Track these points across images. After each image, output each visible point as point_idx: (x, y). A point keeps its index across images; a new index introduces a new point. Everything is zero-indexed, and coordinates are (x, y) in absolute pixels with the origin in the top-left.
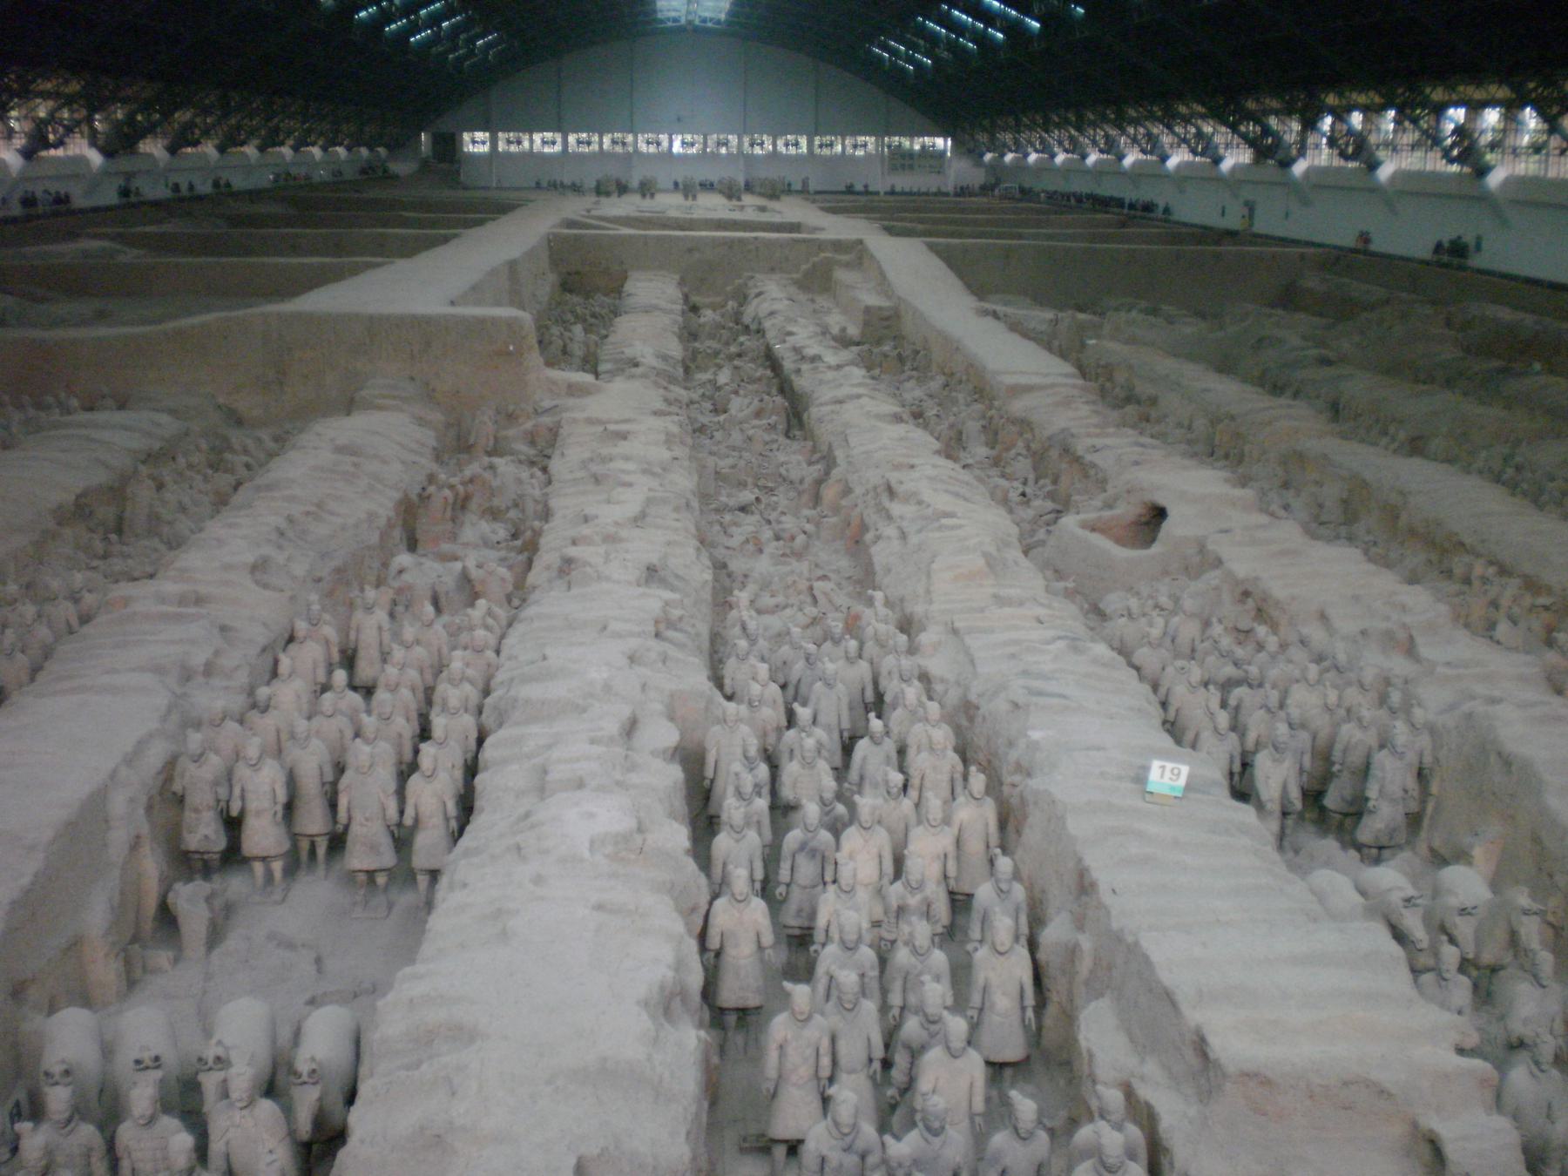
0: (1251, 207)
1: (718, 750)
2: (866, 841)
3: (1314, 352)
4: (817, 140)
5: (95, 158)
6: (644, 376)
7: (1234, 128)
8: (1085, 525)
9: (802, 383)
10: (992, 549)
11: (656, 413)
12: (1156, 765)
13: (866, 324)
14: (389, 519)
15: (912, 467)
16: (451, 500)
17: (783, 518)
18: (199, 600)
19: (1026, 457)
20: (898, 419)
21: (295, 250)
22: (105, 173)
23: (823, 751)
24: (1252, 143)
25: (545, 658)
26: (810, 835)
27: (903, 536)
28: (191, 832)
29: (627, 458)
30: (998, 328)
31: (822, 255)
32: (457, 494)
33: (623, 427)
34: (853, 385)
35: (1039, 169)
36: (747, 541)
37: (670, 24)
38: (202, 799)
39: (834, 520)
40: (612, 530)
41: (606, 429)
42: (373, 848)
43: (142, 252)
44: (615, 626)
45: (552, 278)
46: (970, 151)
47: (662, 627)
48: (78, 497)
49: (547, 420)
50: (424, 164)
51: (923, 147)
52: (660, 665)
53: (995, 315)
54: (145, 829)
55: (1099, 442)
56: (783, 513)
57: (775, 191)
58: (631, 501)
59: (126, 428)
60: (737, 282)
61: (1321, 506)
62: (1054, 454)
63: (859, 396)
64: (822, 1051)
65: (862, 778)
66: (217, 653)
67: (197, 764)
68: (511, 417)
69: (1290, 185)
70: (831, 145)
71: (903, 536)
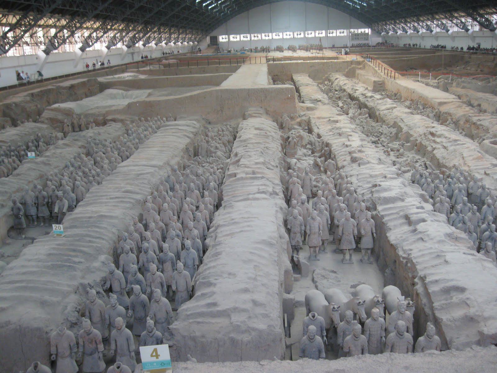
5: (125, 48)
7: (475, 19)
8: (491, 143)
9: (370, 104)
11: (338, 115)
13: (374, 86)
15: (434, 127)
17: (389, 145)
19: (452, 124)
20: (412, 113)
21: (191, 73)
22: (128, 53)
24: (481, 24)
25: (380, 185)
27: (445, 147)
29: (345, 128)
30: (421, 84)
31: (352, 66)
34: (390, 104)
38: (297, 229)
39: (409, 144)
40: (359, 149)
41: (330, 120)
42: (351, 243)
44: (389, 176)
46: (378, 32)
49: (304, 118)
50: (209, 46)
53: (418, 81)
55: (481, 118)
57: (320, 48)
62: (462, 123)
63: (395, 108)
68: (292, 118)
71: (445, 147)
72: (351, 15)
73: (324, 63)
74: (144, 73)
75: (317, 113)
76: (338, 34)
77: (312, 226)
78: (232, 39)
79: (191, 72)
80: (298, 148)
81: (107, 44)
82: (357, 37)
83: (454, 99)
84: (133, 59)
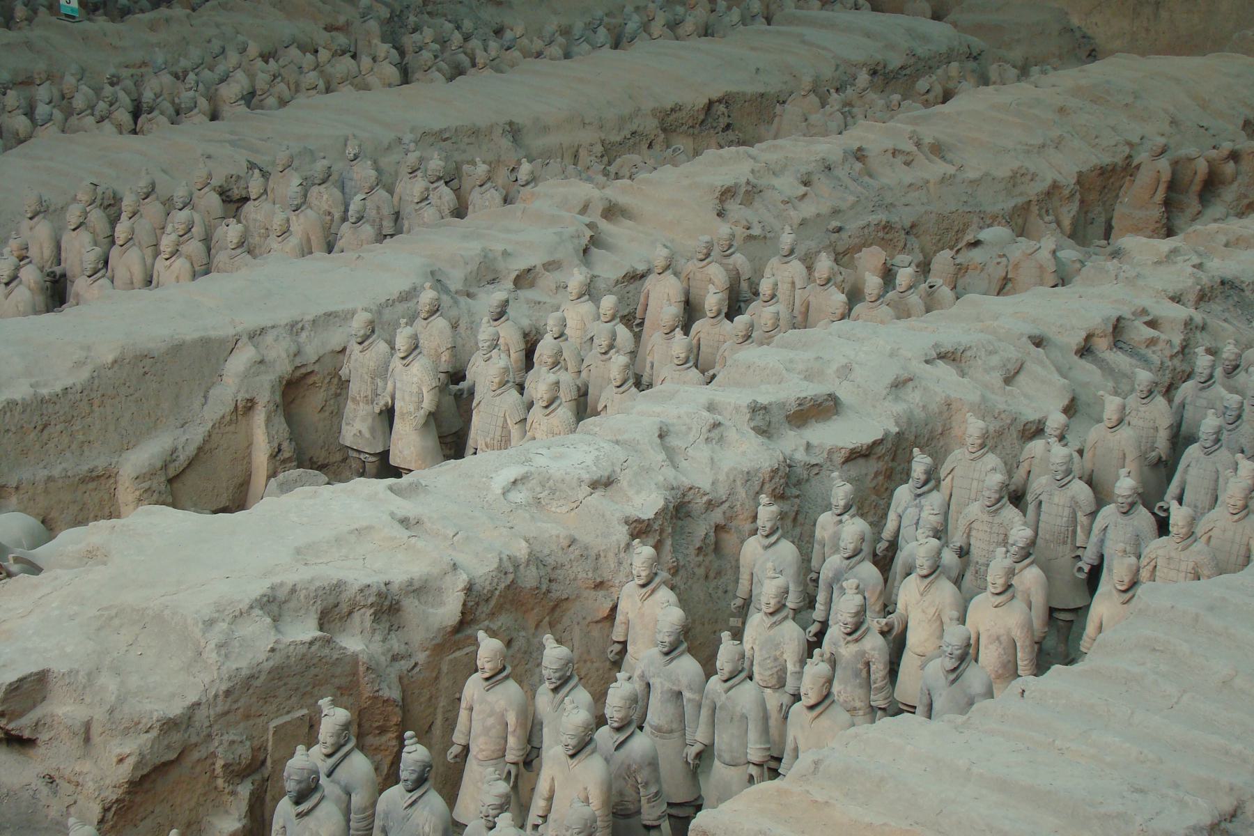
1: (953, 478)
2: (922, 595)
14: (1055, 186)
16: (1166, 176)
18: (612, 212)
23: (1079, 514)
26: (847, 562)
28: (348, 424)
32: (1196, 173)
47: (1101, 344)
48: (711, 104)
54: (265, 397)
59: (868, 35)
64: (510, 729)
65: (1102, 557)
66: (551, 266)
67: (360, 347)
77: (398, 385)
80: (1217, 209)
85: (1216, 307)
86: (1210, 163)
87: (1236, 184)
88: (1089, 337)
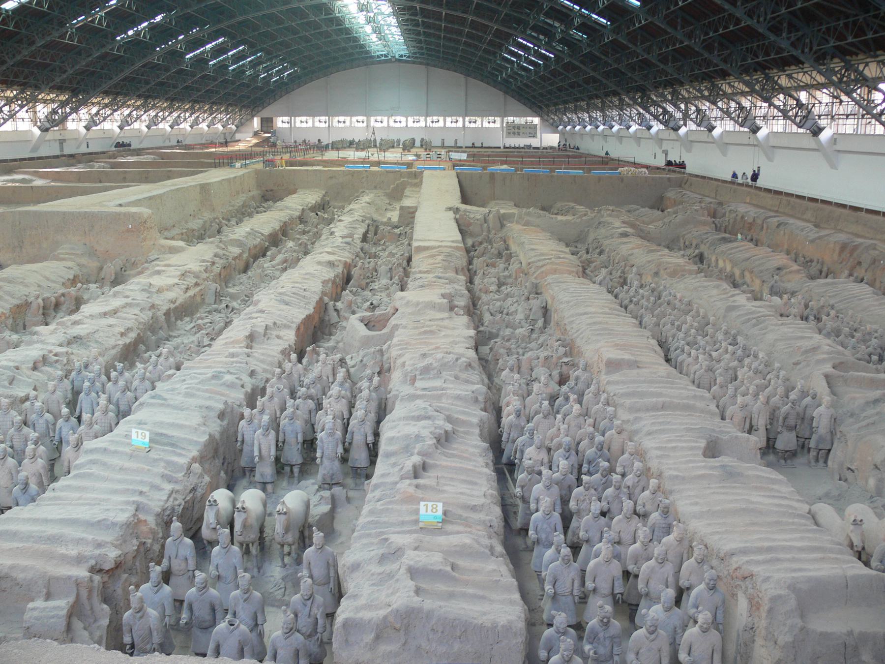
0: (666, 153)
3: (620, 230)
4: (467, 119)
5: (37, 132)
6: (212, 243)
10: (261, 330)
12: (134, 431)
13: (400, 216)
16: (42, 304)
29: (138, 283)
33: (163, 268)
35: (581, 135)
36: (194, 327)
37: (383, 58)
43: (49, 181)
45: (255, 193)
46: (552, 125)
47: (40, 365)
51: (526, 123)
52: (6, 383)
53: (456, 210)
56: (235, 313)
58: (117, 303)
60: (356, 194)
61: (531, 309)
69: (679, 139)
70: (475, 122)
72: (506, 93)
73: (354, 172)
74: (43, 176)
75: (175, 259)
76: (486, 125)
78: (298, 125)
79: (125, 178)
80: (61, 314)
81: (119, 123)
82: (516, 131)
83: (453, 242)
84: (62, 149)
85: (74, 346)
86: (56, 298)
87: (65, 306)
88: (35, 363)
